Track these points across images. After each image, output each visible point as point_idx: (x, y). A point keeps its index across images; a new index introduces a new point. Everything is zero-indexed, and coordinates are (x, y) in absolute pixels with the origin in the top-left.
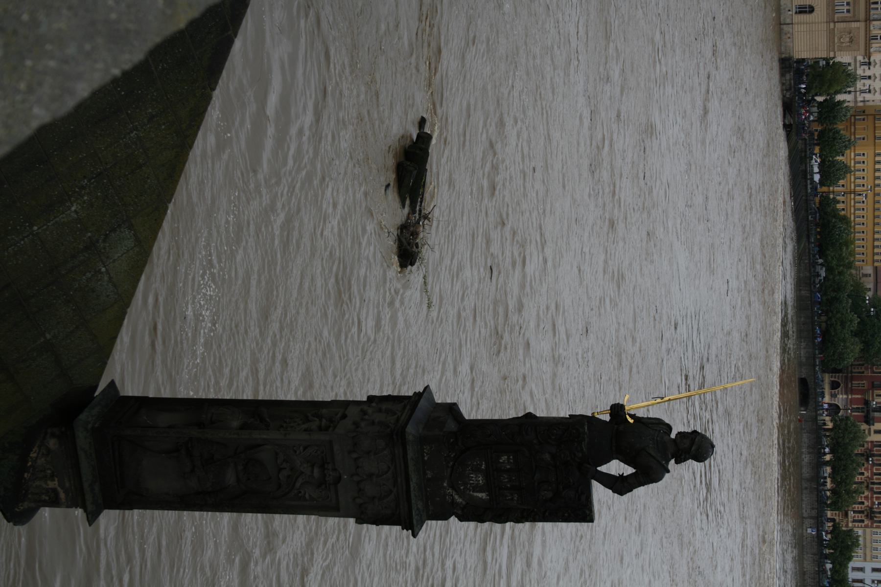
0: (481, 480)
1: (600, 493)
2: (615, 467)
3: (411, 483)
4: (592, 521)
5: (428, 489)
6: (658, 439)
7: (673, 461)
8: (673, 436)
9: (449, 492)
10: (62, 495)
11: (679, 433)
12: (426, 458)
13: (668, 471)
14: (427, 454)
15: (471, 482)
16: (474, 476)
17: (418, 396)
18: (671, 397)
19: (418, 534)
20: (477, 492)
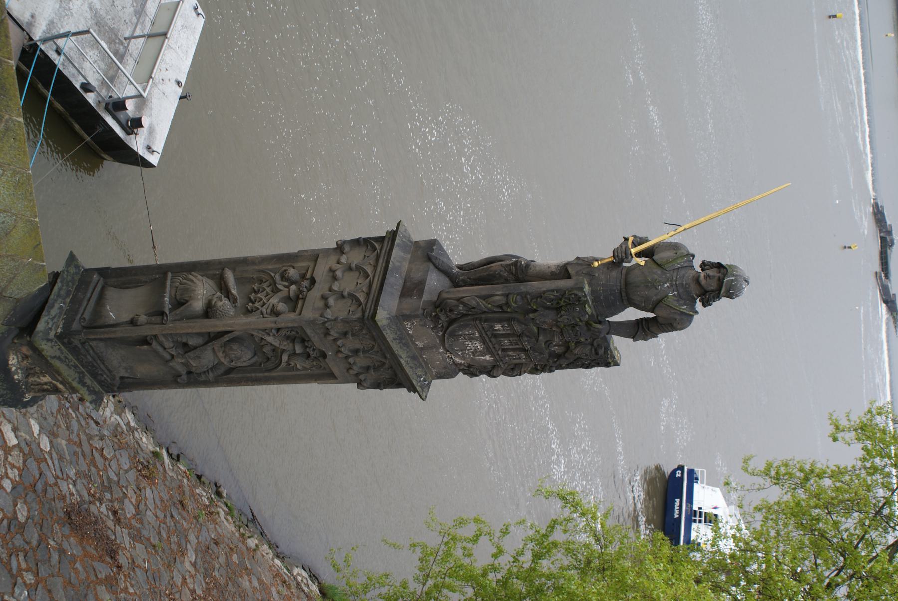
0: (479, 345)
1: (620, 344)
2: (631, 314)
3: (401, 360)
4: (617, 364)
5: (424, 356)
6: (678, 283)
7: (699, 305)
8: (697, 264)
9: (448, 356)
10: (61, 386)
11: (704, 265)
12: (410, 332)
13: (697, 312)
14: (410, 328)
15: (468, 348)
16: (470, 343)
17: (393, 235)
18: (687, 226)
19: (426, 396)
20: (478, 356)
